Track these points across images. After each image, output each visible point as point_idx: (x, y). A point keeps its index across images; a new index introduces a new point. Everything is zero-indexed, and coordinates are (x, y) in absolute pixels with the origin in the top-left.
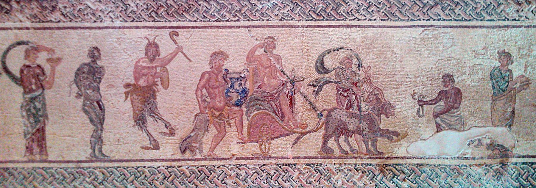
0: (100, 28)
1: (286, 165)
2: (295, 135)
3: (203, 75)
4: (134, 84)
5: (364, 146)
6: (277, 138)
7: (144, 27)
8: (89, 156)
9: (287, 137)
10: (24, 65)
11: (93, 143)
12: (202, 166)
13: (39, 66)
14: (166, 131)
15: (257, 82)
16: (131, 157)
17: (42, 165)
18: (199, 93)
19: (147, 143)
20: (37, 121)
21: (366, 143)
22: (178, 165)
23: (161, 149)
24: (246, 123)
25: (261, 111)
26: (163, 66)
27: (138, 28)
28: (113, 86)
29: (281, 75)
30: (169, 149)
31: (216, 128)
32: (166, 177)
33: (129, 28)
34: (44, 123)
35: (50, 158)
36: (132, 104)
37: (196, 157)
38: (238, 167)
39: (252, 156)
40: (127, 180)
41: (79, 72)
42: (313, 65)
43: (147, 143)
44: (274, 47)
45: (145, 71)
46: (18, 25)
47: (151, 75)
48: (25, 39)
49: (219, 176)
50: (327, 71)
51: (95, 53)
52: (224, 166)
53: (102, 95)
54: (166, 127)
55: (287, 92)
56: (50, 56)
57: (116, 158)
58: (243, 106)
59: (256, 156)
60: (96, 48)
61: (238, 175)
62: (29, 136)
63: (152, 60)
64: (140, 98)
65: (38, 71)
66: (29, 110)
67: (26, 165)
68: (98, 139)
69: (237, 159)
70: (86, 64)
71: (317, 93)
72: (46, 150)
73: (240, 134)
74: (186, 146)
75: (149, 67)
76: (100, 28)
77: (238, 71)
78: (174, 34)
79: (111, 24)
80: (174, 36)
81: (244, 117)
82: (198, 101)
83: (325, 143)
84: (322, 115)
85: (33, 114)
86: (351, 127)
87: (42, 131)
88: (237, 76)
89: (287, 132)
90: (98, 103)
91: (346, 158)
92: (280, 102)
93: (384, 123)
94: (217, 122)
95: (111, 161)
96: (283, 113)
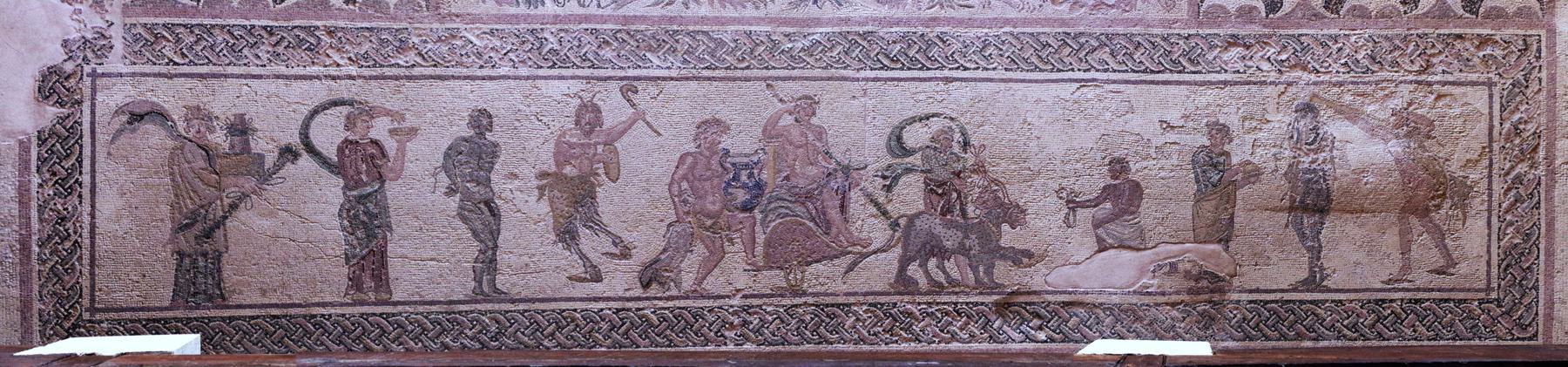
0: (491, 78)
2: (849, 259)
3: (682, 158)
5: (971, 275)
9: (836, 261)
13: (375, 143)
16: (549, 293)
18: (675, 188)
19: (579, 270)
20: (371, 236)
21: (975, 270)
24: (761, 239)
28: (516, 176)
30: (619, 281)
31: (707, 247)
33: (545, 78)
34: (385, 238)
38: (746, 309)
41: (452, 152)
42: (883, 142)
43: (579, 270)
44: (814, 114)
45: (577, 151)
46: (333, 71)
48: (346, 96)
50: (907, 152)
51: (482, 120)
53: (496, 189)
54: (615, 244)
56: (396, 125)
60: (483, 112)
61: (745, 323)
63: (588, 134)
65: (372, 150)
66: (356, 216)
68: (488, 263)
69: (745, 297)
71: (889, 188)
74: (651, 275)
76: (491, 78)
77: (747, 151)
78: (629, 88)
79: (512, 72)
81: (758, 228)
86: (948, 244)
87: (382, 255)
88: (745, 160)
90: (487, 203)
91: (938, 293)
93: (1009, 237)
95: (513, 301)
96: (828, 222)
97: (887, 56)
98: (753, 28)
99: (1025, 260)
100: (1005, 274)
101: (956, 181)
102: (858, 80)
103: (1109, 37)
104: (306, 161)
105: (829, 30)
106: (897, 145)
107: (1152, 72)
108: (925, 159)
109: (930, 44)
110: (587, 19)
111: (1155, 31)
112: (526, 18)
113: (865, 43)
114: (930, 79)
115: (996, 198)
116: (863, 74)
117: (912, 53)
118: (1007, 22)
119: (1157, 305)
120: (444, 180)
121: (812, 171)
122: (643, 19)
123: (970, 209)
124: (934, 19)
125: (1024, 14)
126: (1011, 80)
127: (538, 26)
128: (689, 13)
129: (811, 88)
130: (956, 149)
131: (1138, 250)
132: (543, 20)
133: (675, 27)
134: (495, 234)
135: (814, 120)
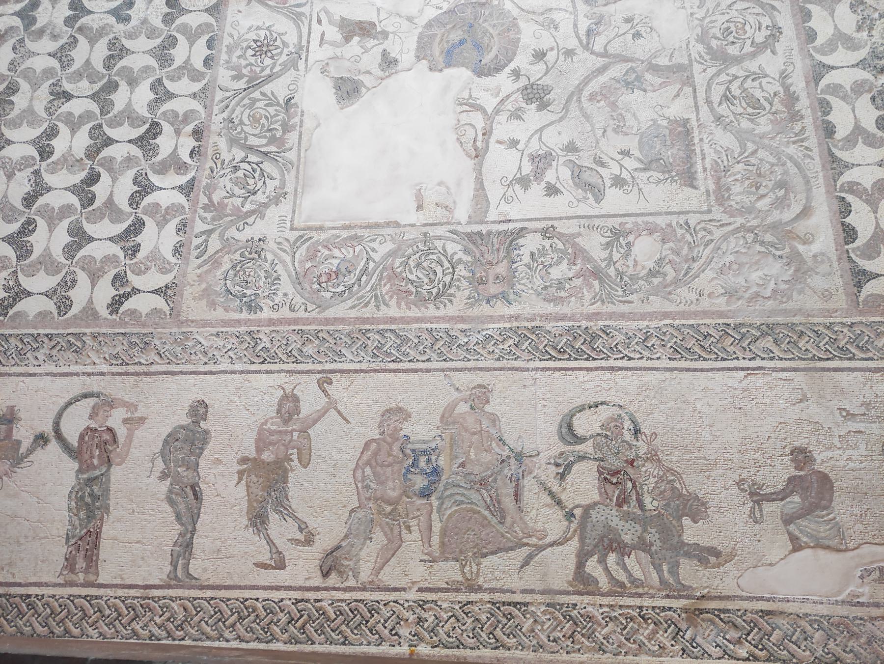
0: (212, 373)
1: (509, 604)
2: (525, 551)
3: (367, 445)
4: (255, 458)
5: (655, 575)
6: (493, 553)
7: (278, 372)
8: (165, 577)
9: (511, 554)
10: (88, 428)
11: (175, 555)
12: (356, 601)
13: (110, 430)
14: (298, 538)
15: (457, 457)
16: (236, 581)
17: (84, 591)
18: (359, 474)
20: (90, 517)
21: (659, 571)
22: (315, 597)
23: (288, 568)
24: (437, 526)
25: (464, 506)
26: (304, 431)
27: (270, 372)
29: (498, 445)
30: (302, 568)
31: (386, 535)
32: (293, 619)
33: (256, 372)
34: (102, 519)
35: (101, 581)
36: (248, 490)
37: (346, 584)
38: (422, 604)
39: (446, 586)
40: (224, 623)
41: (171, 439)
42: (554, 428)
43: (265, 558)
44: (488, 402)
46: (89, 369)
47: (284, 445)
48: (96, 389)
49: (386, 621)
50: (580, 440)
51: (199, 410)
52: (396, 602)
54: (301, 530)
55: (509, 475)
57: (211, 582)
58: (433, 498)
59: (454, 587)
61: (420, 621)
62: (73, 541)
63: (286, 422)
64: (261, 480)
65: (107, 437)
66: (82, 498)
67: (58, 591)
68: (185, 547)
69: (420, 590)
70: (182, 427)
71: (562, 476)
72: (97, 565)
73: (427, 545)
74: (330, 564)
75: (280, 432)
76: (212, 373)
78: (324, 383)
79: (230, 367)
80: (325, 384)
81: (435, 516)
82: (357, 486)
83: (580, 565)
84: (573, 515)
85: (87, 504)
86: (627, 538)
87: (96, 535)
88: (424, 447)
89: (510, 544)
90: (193, 488)
91: (621, 595)
92: (497, 490)
93: (692, 532)
94: (387, 524)
95: (202, 588)
96: (502, 511)
97: (555, 348)
98: (434, 326)
99: (713, 559)
100: (691, 573)
101: (630, 470)
102: (528, 370)
103: (771, 327)
104: (54, 446)
105: (501, 325)
106: (568, 432)
107: (820, 359)
108: (596, 446)
109: (594, 337)
110: (295, 321)
111: (817, 320)
112: (246, 322)
113: (533, 337)
114: (596, 369)
115: (673, 488)
116: (532, 365)
117: (578, 345)
118: (666, 315)
119: (873, 619)
120: (160, 465)
121: (486, 457)
122: (342, 320)
123: (647, 500)
124: (597, 314)
125: (682, 307)
126: (676, 369)
127: (255, 329)
128: (379, 314)
129: (485, 378)
130: (628, 436)
131: (839, 551)
132: (259, 323)
133: (368, 327)
134: (195, 517)
135: (488, 408)
